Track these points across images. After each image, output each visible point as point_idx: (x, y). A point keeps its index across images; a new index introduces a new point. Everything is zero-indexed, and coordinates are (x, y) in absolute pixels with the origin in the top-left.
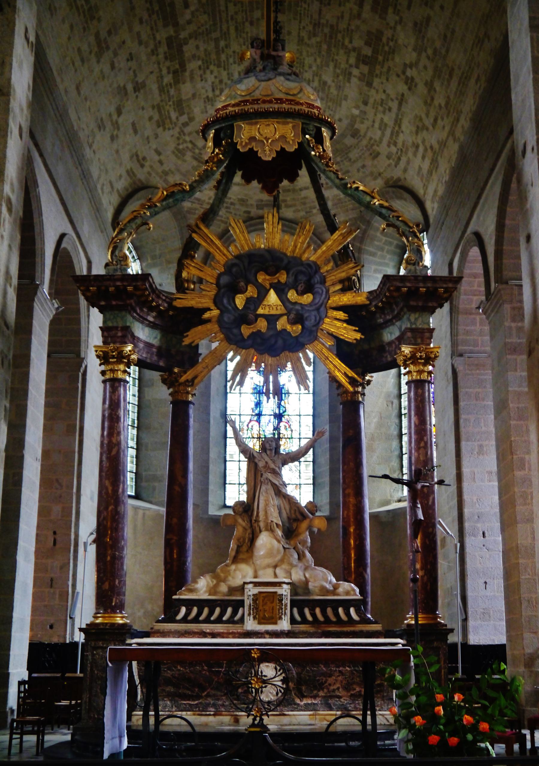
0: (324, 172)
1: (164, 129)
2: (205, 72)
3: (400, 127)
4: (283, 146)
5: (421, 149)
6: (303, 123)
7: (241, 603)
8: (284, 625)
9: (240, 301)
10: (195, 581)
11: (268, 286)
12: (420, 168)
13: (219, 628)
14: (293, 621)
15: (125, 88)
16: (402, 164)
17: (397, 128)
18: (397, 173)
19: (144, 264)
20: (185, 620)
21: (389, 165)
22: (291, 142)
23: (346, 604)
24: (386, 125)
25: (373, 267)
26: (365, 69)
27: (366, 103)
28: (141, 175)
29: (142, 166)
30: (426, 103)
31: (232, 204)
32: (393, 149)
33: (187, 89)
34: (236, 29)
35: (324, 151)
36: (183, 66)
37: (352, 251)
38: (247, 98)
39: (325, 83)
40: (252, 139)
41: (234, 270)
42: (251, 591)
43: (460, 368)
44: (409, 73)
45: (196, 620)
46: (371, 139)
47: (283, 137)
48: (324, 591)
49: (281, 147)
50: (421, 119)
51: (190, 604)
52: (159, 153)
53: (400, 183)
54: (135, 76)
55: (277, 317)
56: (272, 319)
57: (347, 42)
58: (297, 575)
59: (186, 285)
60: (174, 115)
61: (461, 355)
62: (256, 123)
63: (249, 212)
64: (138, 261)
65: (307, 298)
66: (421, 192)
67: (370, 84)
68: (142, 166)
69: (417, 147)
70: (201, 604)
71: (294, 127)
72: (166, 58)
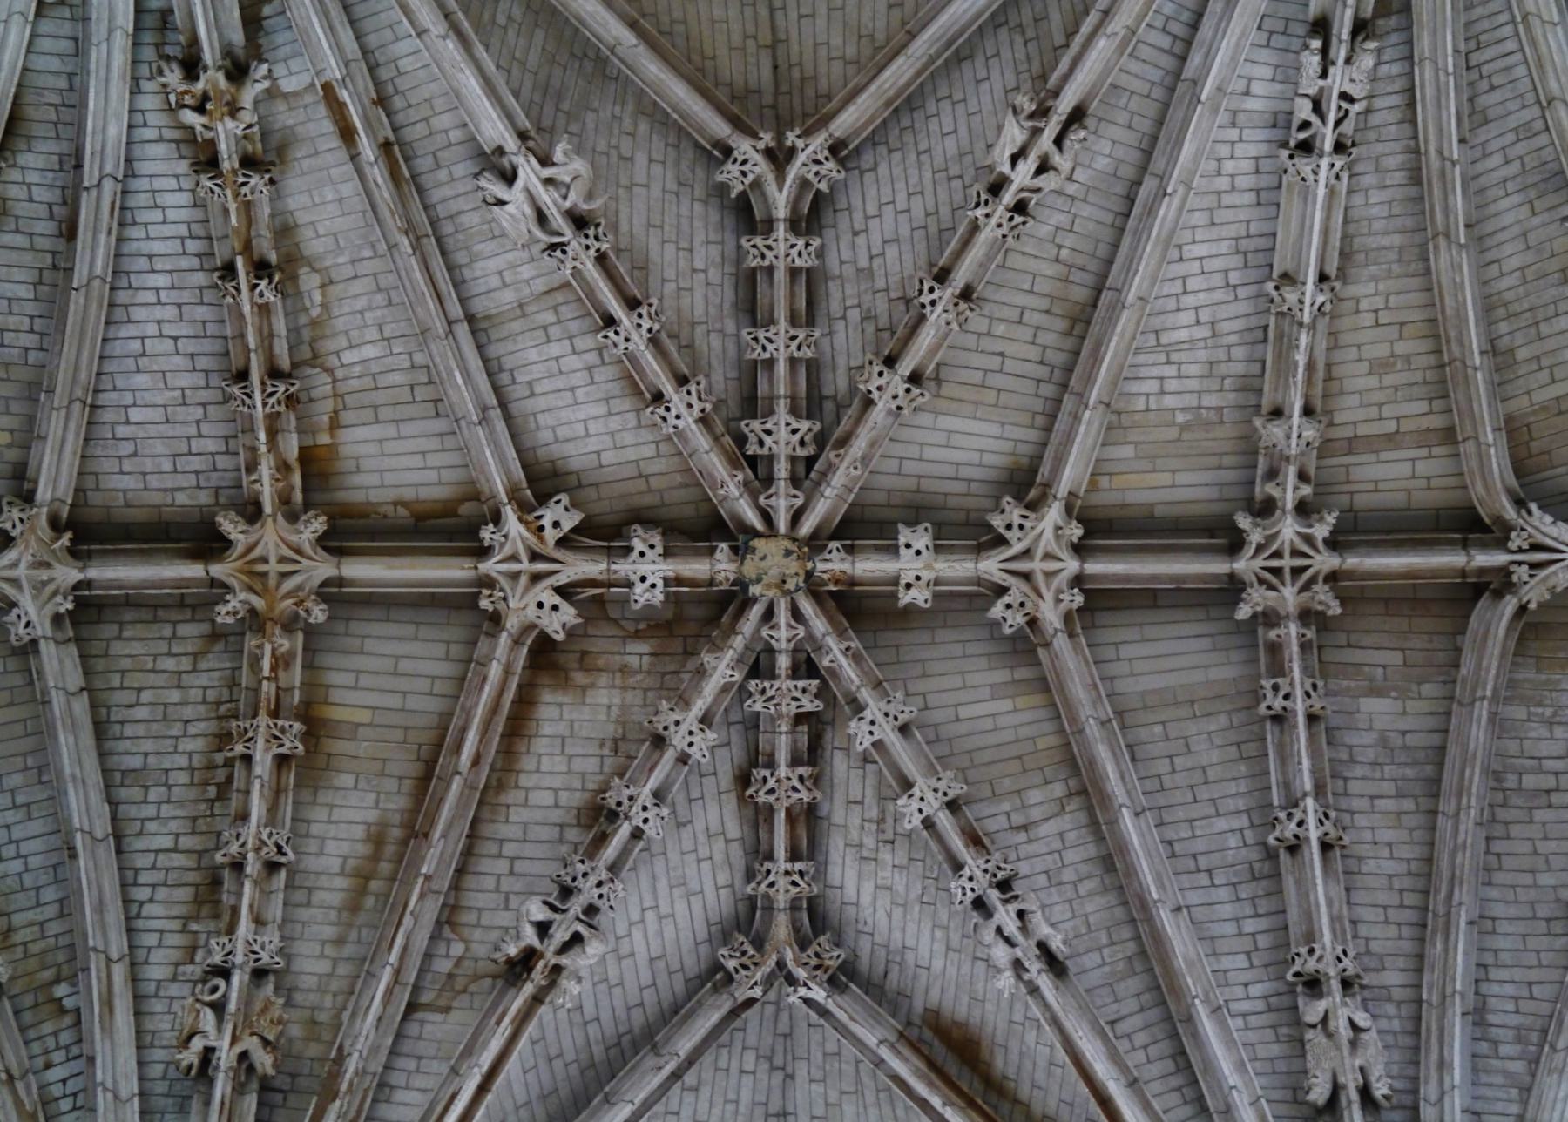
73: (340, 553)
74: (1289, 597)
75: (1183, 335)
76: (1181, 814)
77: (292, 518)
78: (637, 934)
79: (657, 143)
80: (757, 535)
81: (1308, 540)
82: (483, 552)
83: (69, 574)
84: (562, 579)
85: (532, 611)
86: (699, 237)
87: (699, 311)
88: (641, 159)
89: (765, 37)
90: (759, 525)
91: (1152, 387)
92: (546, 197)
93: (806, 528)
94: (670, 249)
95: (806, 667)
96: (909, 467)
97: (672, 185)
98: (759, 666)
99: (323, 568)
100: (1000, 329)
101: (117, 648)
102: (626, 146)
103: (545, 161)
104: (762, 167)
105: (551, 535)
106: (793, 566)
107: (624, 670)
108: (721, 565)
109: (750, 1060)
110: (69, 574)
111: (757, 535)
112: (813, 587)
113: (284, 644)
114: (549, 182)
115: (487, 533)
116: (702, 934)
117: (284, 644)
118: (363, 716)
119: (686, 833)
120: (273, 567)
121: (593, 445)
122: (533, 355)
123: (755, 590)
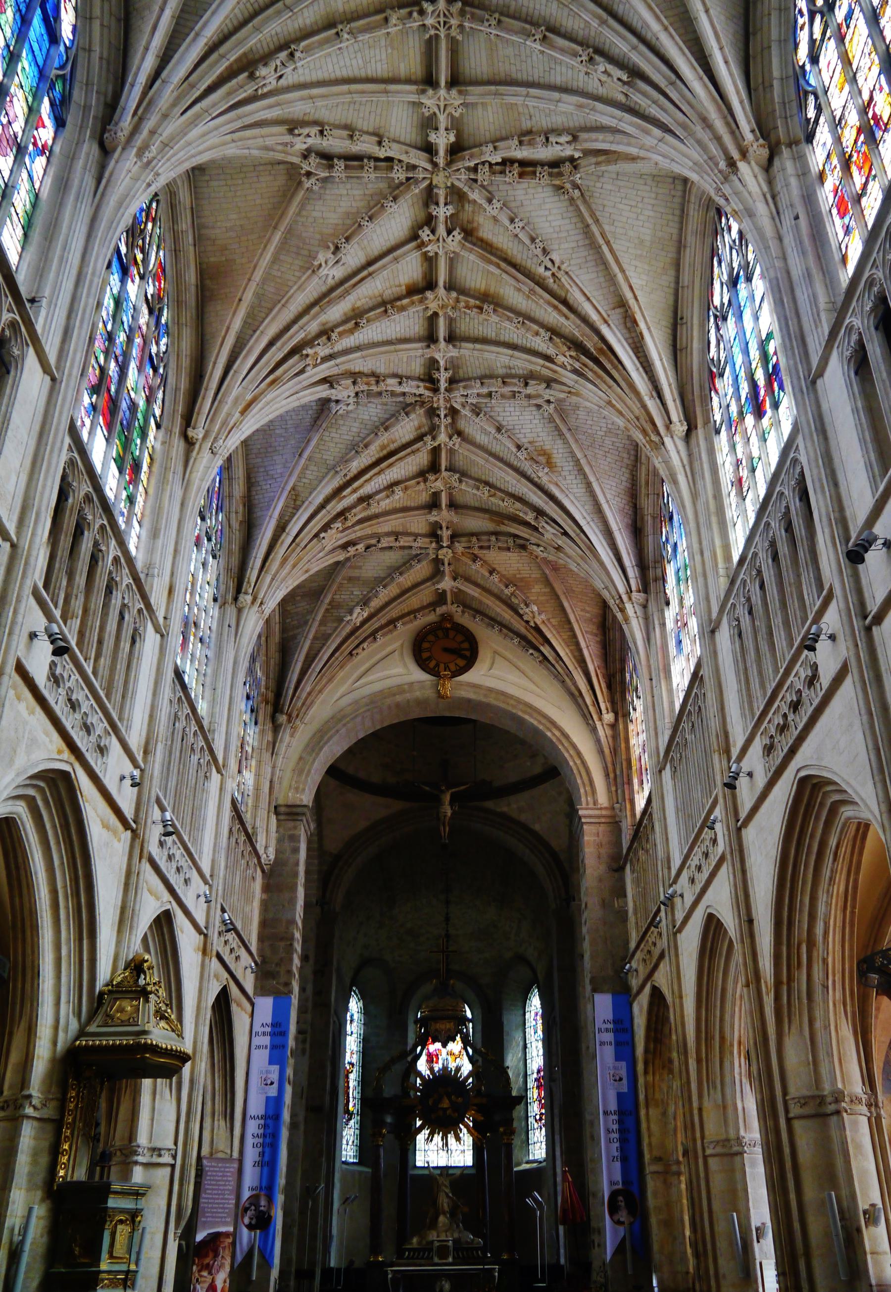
7: (432, 1249)
8: (450, 1260)
9: (430, 1102)
10: (412, 1238)
13: (423, 1262)
14: (454, 1258)
20: (408, 1258)
23: (477, 1249)
42: (437, 1244)
45: (413, 1258)
47: (449, 1030)
48: (467, 1242)
51: (410, 1250)
55: (446, 1109)
56: (445, 1110)
58: (456, 1235)
65: (460, 1100)
70: (414, 1250)
73: (436, 285)
74: (454, 22)
75: (360, 61)
76: (530, 69)
77: (426, 299)
78: (554, 224)
79: (309, 207)
80: (431, 183)
81: (433, 12)
82: (436, 254)
83: (442, 344)
84: (445, 234)
85: (454, 244)
86: (337, 192)
87: (361, 192)
88: (315, 214)
89: (269, 167)
90: (428, 182)
91: (379, 64)
92: (330, 263)
93: (429, 167)
94: (342, 204)
95: (475, 169)
96: (409, 130)
97: (321, 202)
98: (475, 181)
99: (441, 291)
100: (361, 115)
101: (463, 329)
102: (311, 220)
103: (320, 265)
104: (313, 180)
105: (432, 237)
106: (441, 174)
107: (473, 212)
108: (441, 194)
109: (599, 185)
110: (442, 344)
111: (431, 183)
112: (449, 164)
113: (462, 304)
114: (326, 262)
115: (431, 254)
116: (556, 198)
117: (462, 304)
118: (484, 282)
119: (525, 203)
120: (440, 303)
121: (404, 220)
122: (377, 243)
123: (449, 184)
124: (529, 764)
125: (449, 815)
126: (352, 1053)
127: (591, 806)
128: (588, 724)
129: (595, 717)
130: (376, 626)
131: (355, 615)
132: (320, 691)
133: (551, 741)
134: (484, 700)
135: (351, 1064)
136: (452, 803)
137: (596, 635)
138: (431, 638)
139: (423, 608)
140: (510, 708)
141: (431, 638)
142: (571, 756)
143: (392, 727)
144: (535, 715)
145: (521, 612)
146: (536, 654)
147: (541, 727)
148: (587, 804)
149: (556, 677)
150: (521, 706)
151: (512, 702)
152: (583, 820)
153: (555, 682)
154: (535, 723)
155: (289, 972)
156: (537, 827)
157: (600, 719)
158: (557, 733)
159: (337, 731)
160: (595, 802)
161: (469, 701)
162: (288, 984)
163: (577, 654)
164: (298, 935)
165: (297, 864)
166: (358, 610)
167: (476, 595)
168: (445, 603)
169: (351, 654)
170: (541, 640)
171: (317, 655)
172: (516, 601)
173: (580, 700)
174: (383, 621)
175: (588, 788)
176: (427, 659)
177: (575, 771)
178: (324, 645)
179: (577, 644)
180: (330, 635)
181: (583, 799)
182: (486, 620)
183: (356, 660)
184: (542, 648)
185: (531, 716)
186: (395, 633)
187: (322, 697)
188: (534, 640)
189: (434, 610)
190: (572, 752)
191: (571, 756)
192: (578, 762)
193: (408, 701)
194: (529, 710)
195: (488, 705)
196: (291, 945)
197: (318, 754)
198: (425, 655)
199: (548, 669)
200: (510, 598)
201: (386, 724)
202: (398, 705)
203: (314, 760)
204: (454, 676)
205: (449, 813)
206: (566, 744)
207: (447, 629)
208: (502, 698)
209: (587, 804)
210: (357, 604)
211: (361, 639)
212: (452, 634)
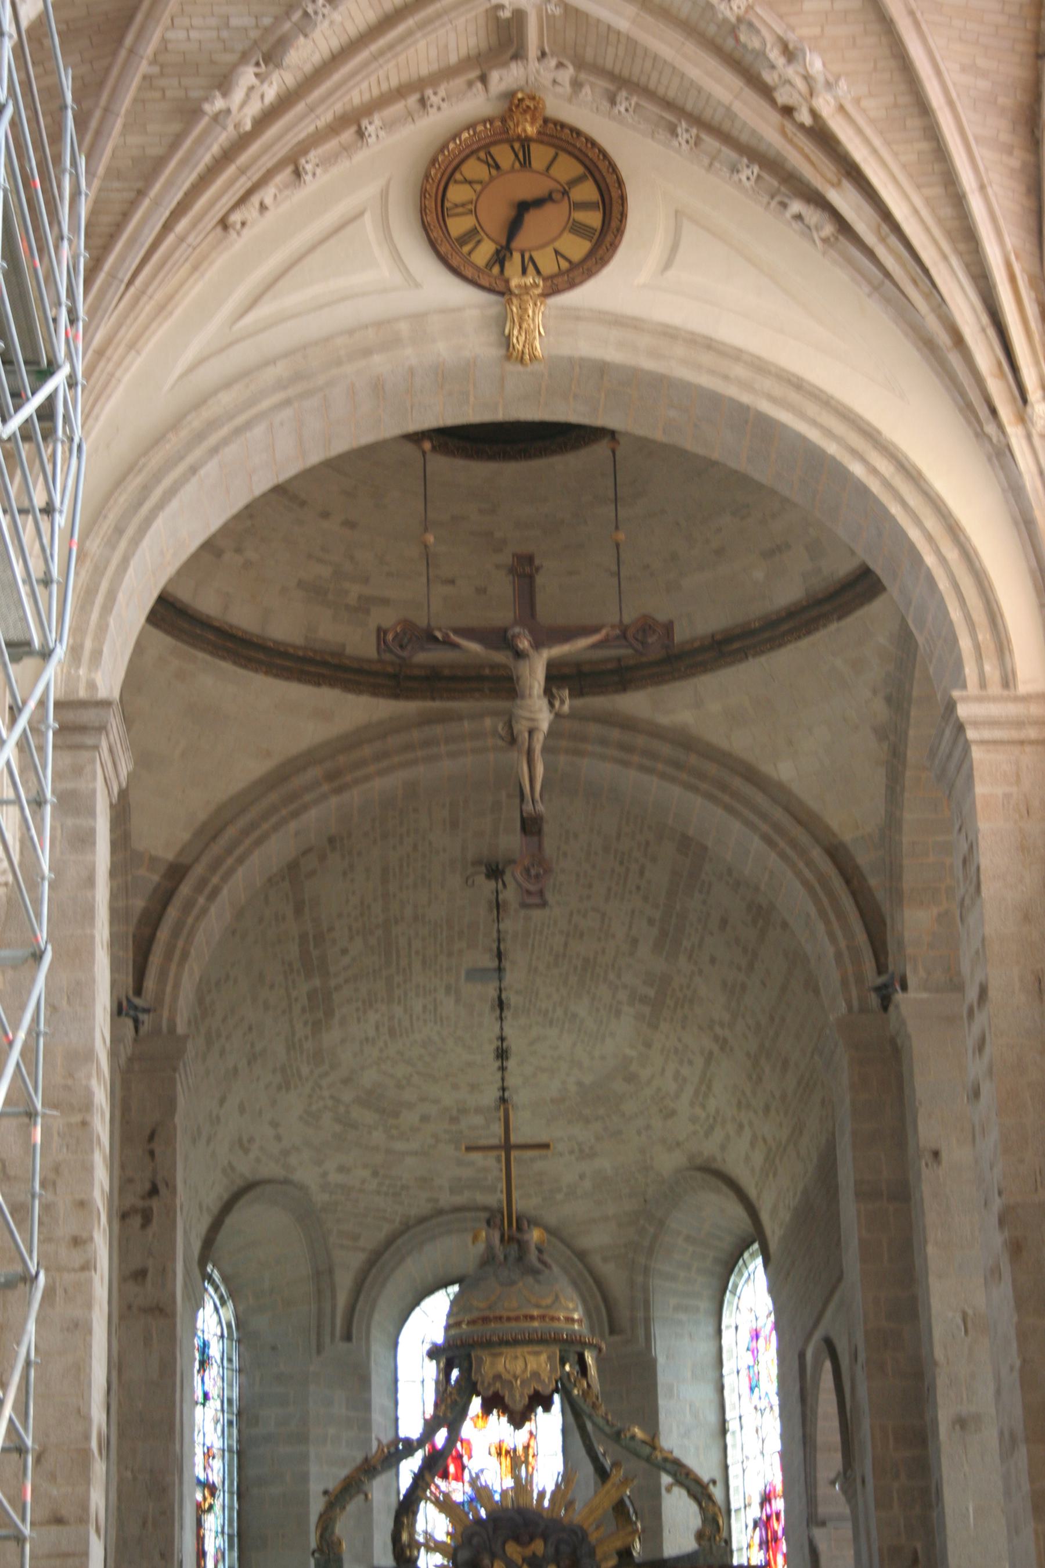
0: (590, 1417)
1: (288, 1089)
2: (365, 1012)
3: (709, 1087)
4: (536, 1387)
5: (747, 1132)
6: (560, 1351)
11: (520, 1561)
12: (747, 1159)
15: (236, 1070)
16: (718, 1135)
17: (704, 1088)
18: (709, 1147)
19: (241, 1308)
21: (695, 1133)
22: (546, 1380)
24: (685, 1080)
25: (673, 1301)
26: (647, 1010)
27: (648, 1045)
28: (245, 1168)
29: (246, 1151)
30: (750, 1077)
31: (405, 1187)
32: (698, 1110)
33: (331, 1037)
34: (424, 962)
35: (589, 1385)
36: (329, 1014)
37: (629, 1497)
38: (487, 1313)
39: (574, 1016)
40: (498, 1377)
41: (475, 1541)
43: (822, 1547)
44: (718, 1029)
46: (659, 1089)
47: (536, 1375)
49: (534, 1388)
50: (744, 1093)
52: (274, 1124)
53: (714, 1166)
54: (252, 1045)
57: (612, 976)
59: (408, 1553)
60: (305, 1070)
61: (823, 1524)
62: (501, 1354)
63: (437, 1201)
64: (230, 1304)
66: (752, 1192)
67: (654, 1027)
68: (246, 1151)
69: (741, 1127)
71: (549, 1358)
72: (303, 1010)
124: (759, 575)
125: (545, 726)
126: (208, 1454)
127: (995, 688)
128: (981, 435)
129: (1005, 413)
130: (307, 129)
131: (238, 95)
132: (132, 346)
133: (863, 491)
134: (649, 364)
135: (212, 1489)
136: (548, 692)
137: (1009, 150)
138: (474, 169)
139: (448, 73)
140: (732, 391)
141: (474, 169)
142: (930, 538)
143: (334, 465)
144: (812, 409)
145: (769, 77)
146: (813, 215)
147: (832, 449)
148: (983, 684)
149: (876, 288)
150: (767, 384)
151: (739, 371)
152: (971, 734)
153: (874, 307)
154: (813, 435)
155: (83, 1205)
156: (784, 771)
157: (1022, 418)
158: (884, 466)
159: (193, 470)
160: (1008, 680)
161: (602, 369)
162: (78, 1242)
163: (947, 211)
164: (101, 1097)
165: (90, 882)
166: (247, 76)
167: (622, 24)
168: (519, 55)
169: (224, 224)
170: (829, 169)
171: (119, 227)
172: (755, 43)
173: (954, 359)
174: (325, 117)
175: (984, 636)
176: (463, 240)
177: (943, 584)
178: (141, 193)
179: (950, 180)
180: (160, 162)
181: (970, 670)
182: (653, 109)
183: (238, 243)
184: (834, 197)
185: (802, 415)
186: (361, 156)
187: (137, 363)
188: (808, 173)
189: (483, 79)
190: (931, 523)
191: (930, 538)
192: (952, 555)
193: (412, 372)
194: (793, 396)
195: (659, 383)
196: (84, 1124)
197: (136, 542)
198: (458, 226)
199: (850, 261)
200: (734, 31)
201: (340, 446)
202: (378, 387)
203: (125, 561)
204: (552, 290)
205: (544, 719)
206: (913, 500)
207: (525, 142)
208: (707, 358)
209: (983, 684)
210: (244, 58)
211: (255, 174)
212: (540, 155)
